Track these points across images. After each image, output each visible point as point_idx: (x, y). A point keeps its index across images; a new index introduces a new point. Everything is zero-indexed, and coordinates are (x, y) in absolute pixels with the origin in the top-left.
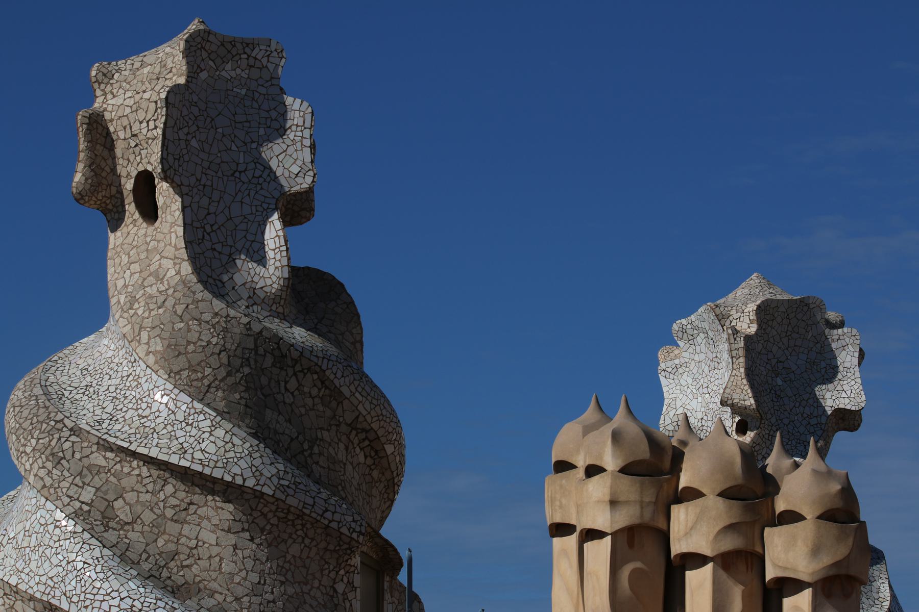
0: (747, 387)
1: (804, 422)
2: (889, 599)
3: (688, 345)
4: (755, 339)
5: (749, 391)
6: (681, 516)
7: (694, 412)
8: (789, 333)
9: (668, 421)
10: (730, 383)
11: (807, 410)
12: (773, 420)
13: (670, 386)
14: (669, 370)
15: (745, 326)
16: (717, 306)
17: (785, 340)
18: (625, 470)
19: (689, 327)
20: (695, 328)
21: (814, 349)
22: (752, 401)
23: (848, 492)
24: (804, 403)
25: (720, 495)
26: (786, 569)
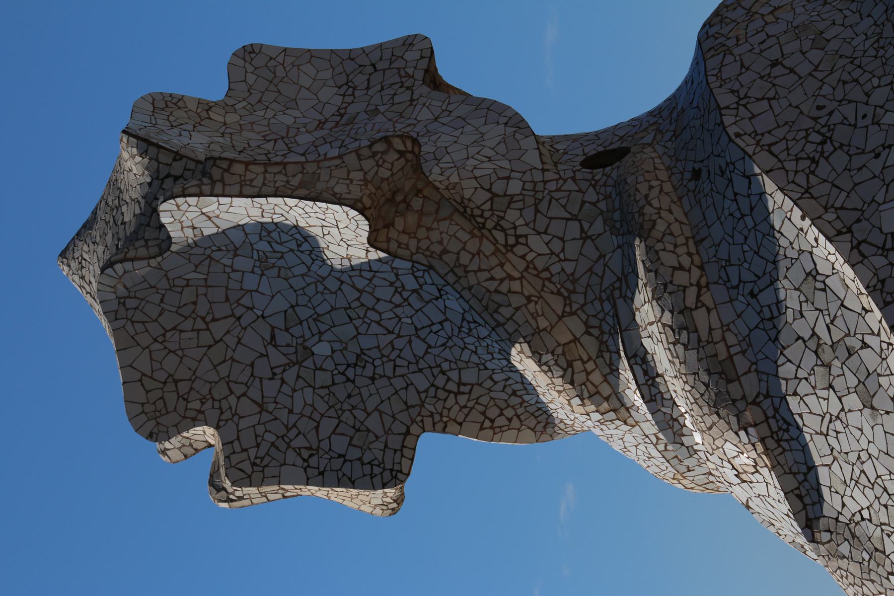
1: (413, 299)
8: (200, 324)
11: (385, 293)
12: (421, 381)
17: (218, 329)
21: (228, 262)
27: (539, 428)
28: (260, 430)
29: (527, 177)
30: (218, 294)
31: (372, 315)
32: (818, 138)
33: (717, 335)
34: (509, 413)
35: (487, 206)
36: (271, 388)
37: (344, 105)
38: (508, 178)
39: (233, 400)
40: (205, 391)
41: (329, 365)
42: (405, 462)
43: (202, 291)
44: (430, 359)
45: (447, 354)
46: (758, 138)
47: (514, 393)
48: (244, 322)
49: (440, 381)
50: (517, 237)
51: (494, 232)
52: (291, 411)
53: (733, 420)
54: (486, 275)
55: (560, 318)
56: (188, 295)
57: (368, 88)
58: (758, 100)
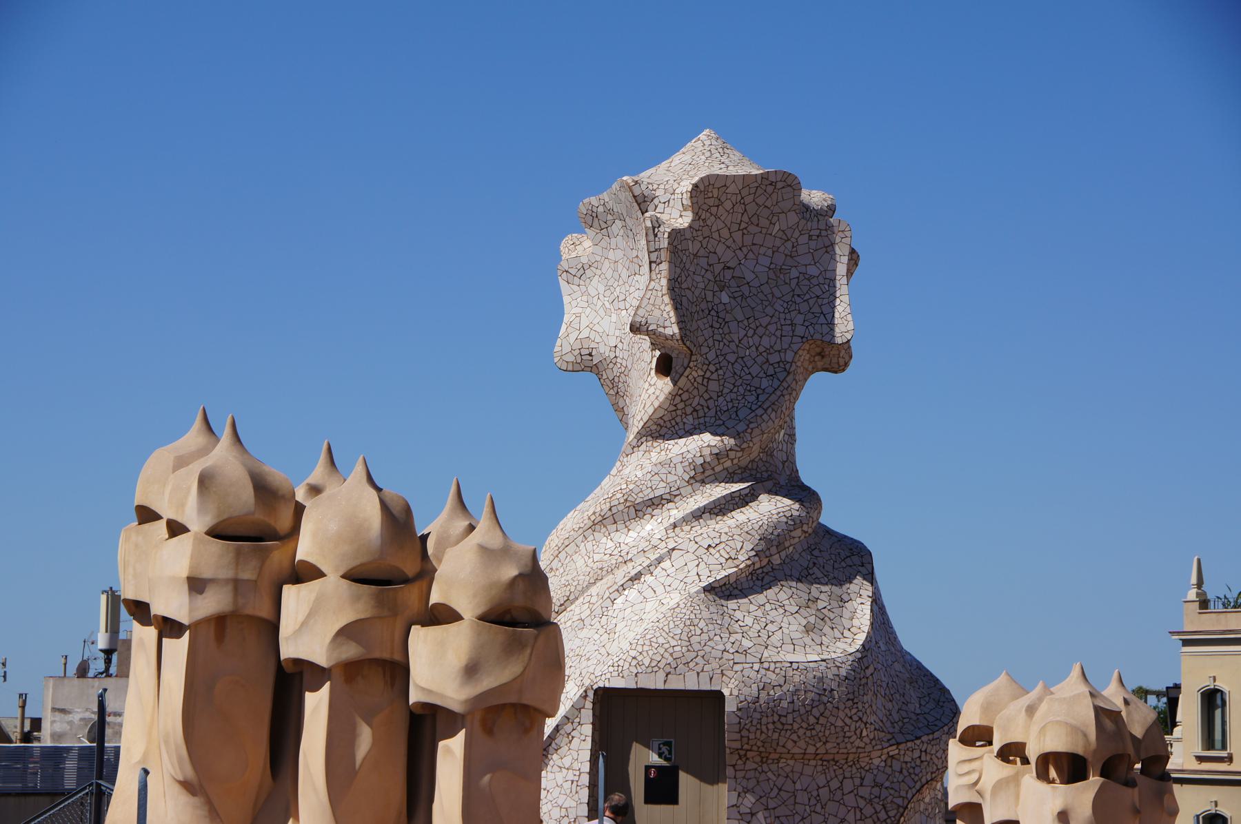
0: (669, 308)
1: (760, 360)
2: (866, 629)
3: (600, 236)
4: (688, 235)
5: (672, 314)
6: (295, 600)
7: (604, 336)
9: (567, 349)
10: (645, 301)
11: (766, 342)
12: (711, 356)
13: (574, 296)
14: (573, 271)
15: (676, 214)
16: (636, 182)
18: (216, 533)
19: (601, 209)
20: (609, 211)
22: (675, 329)
23: (534, 578)
24: (760, 331)
25: (343, 577)
26: (430, 692)
27: (661, 422)
30: (758, 240)
31: (751, 333)
34: (681, 406)
36: (703, 262)
40: (709, 223)
41: (716, 301)
43: (764, 231)
44: (724, 363)
45: (728, 374)
47: (695, 410)
48: (738, 252)
49: (712, 368)
53: (760, 548)
56: (764, 222)
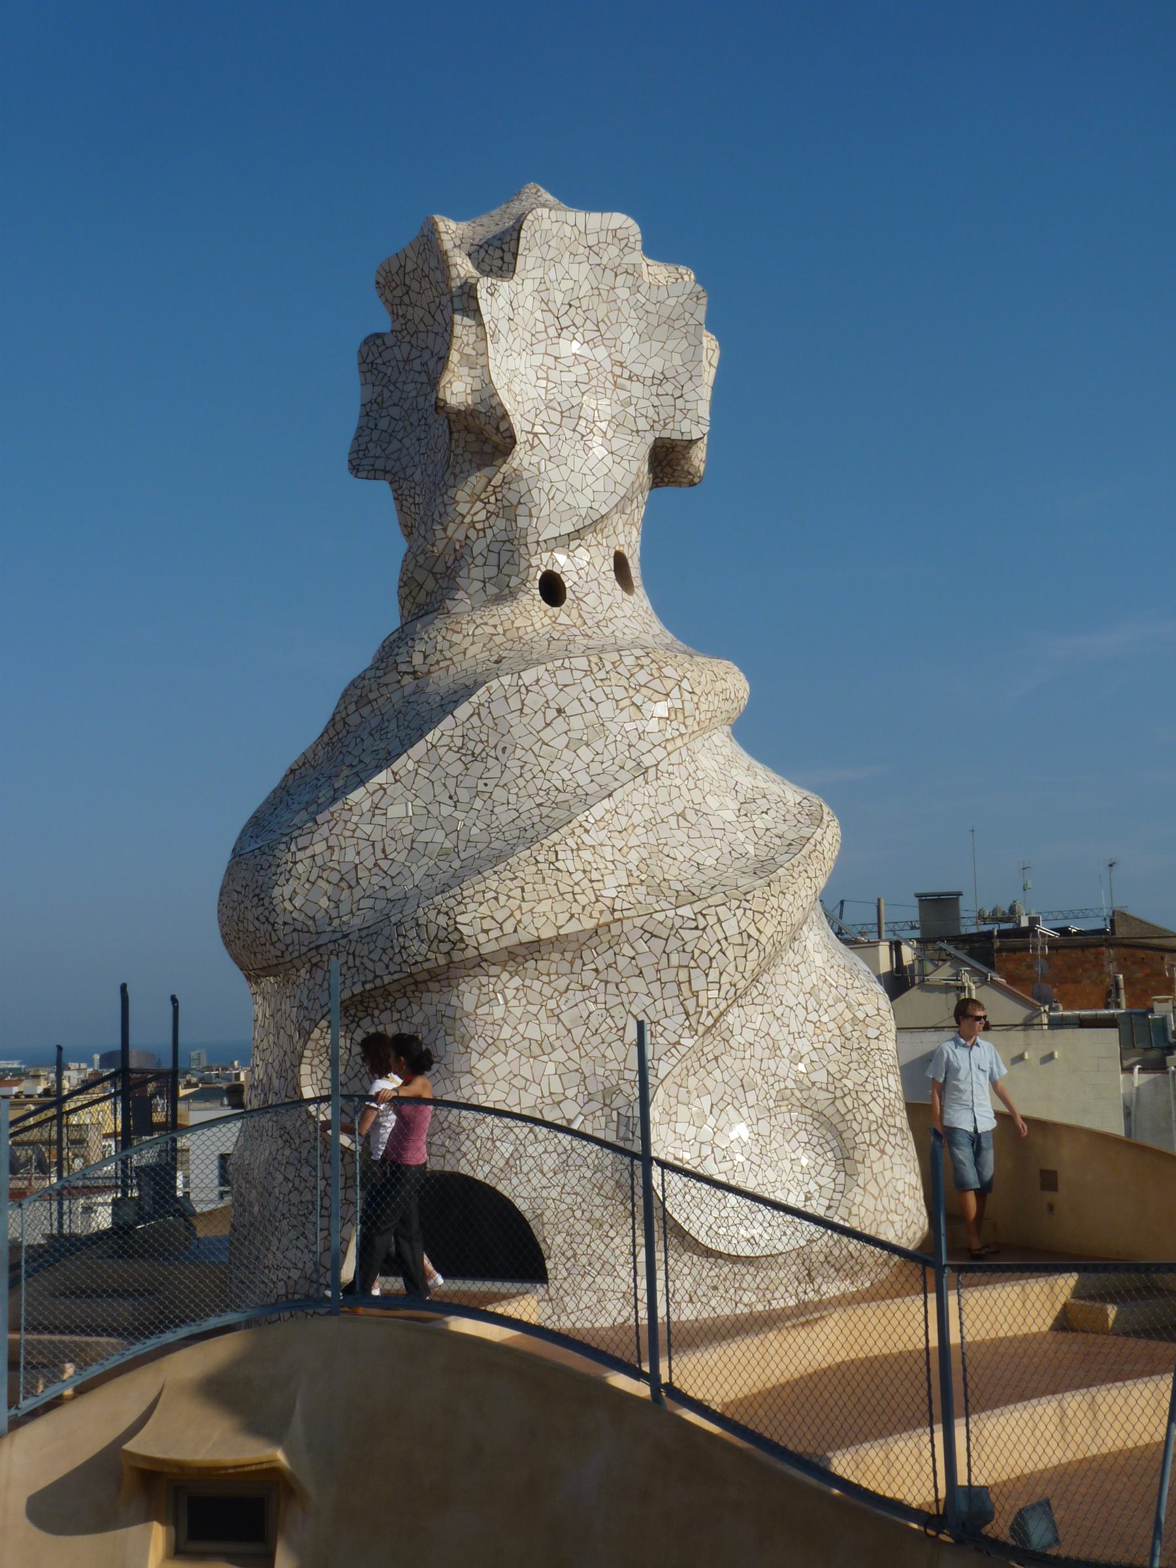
28: (393, 363)
29: (530, 530)
32: (477, 752)
33: (384, 690)
35: (506, 503)
36: (416, 365)
37: (641, 379)
38: (531, 516)
39: (408, 338)
42: (364, 474)
46: (486, 705)
50: (483, 530)
51: (484, 511)
52: (404, 383)
54: (442, 511)
55: (431, 571)
57: (658, 395)
58: (522, 701)
